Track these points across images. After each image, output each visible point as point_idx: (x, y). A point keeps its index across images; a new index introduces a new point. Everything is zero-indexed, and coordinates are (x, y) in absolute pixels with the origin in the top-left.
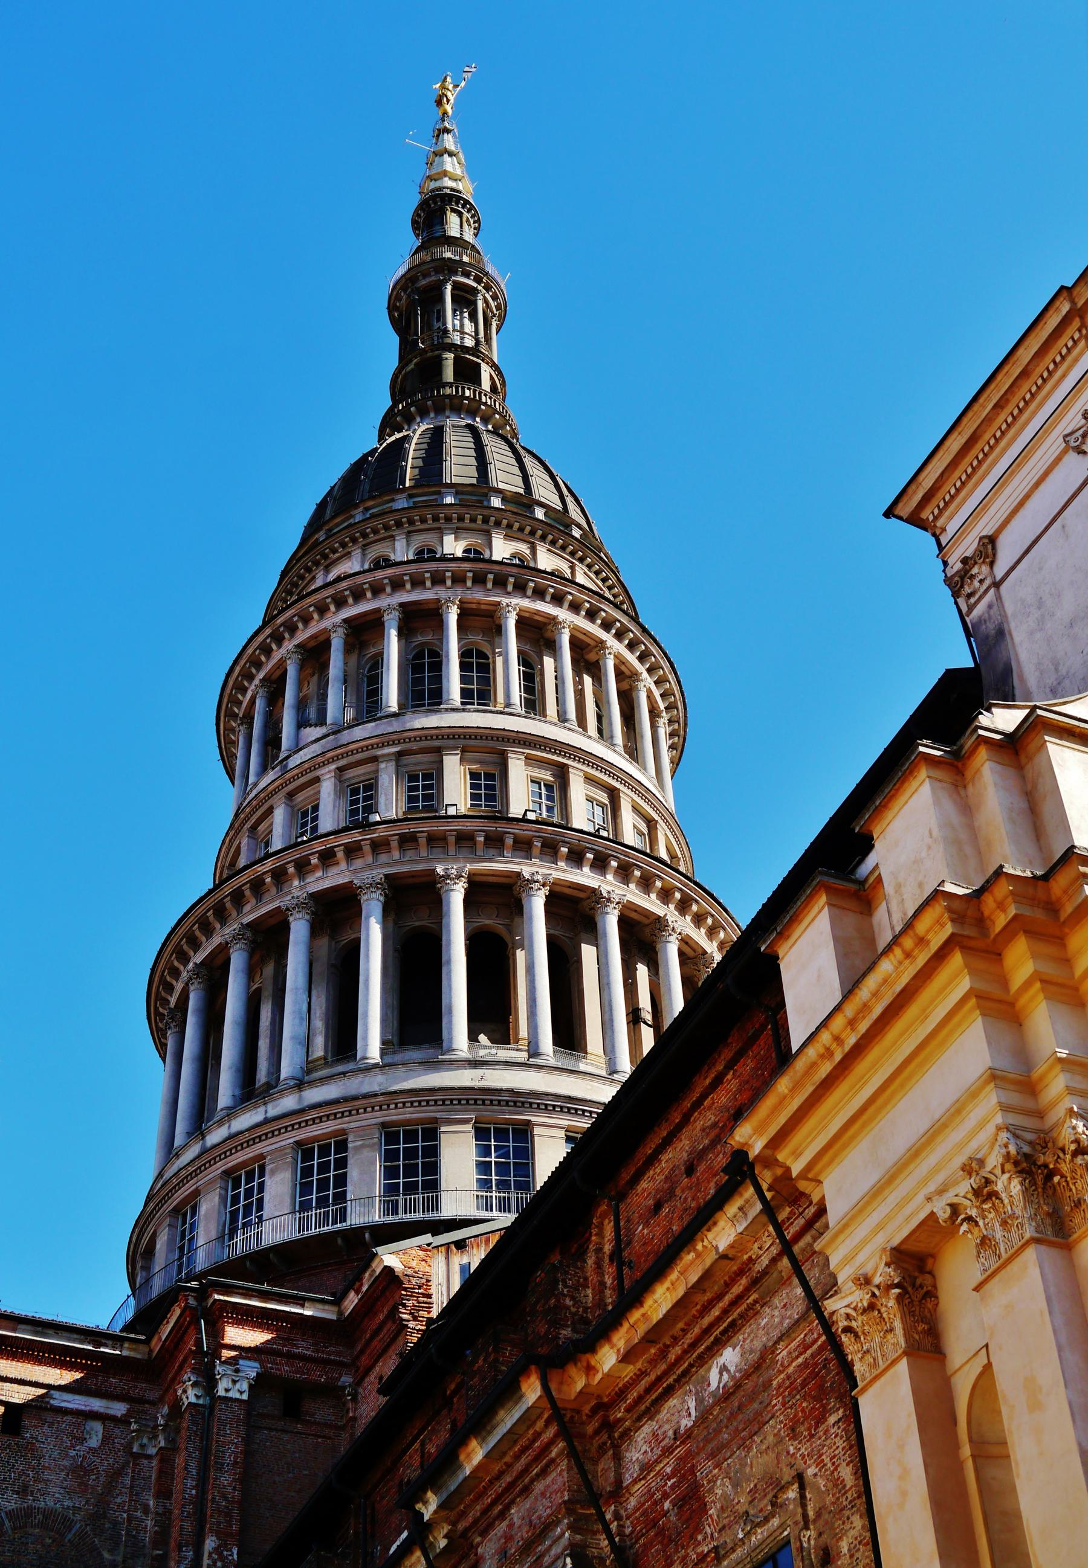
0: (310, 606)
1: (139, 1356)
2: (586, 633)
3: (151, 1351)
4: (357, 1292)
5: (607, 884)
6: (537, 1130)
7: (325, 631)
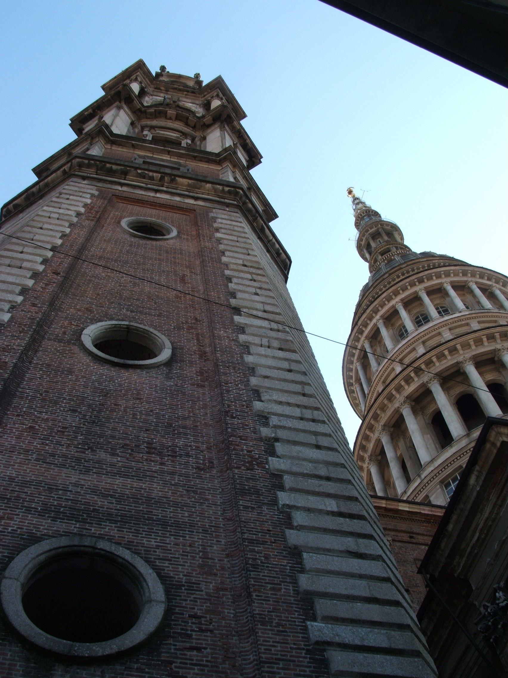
2: (458, 282)
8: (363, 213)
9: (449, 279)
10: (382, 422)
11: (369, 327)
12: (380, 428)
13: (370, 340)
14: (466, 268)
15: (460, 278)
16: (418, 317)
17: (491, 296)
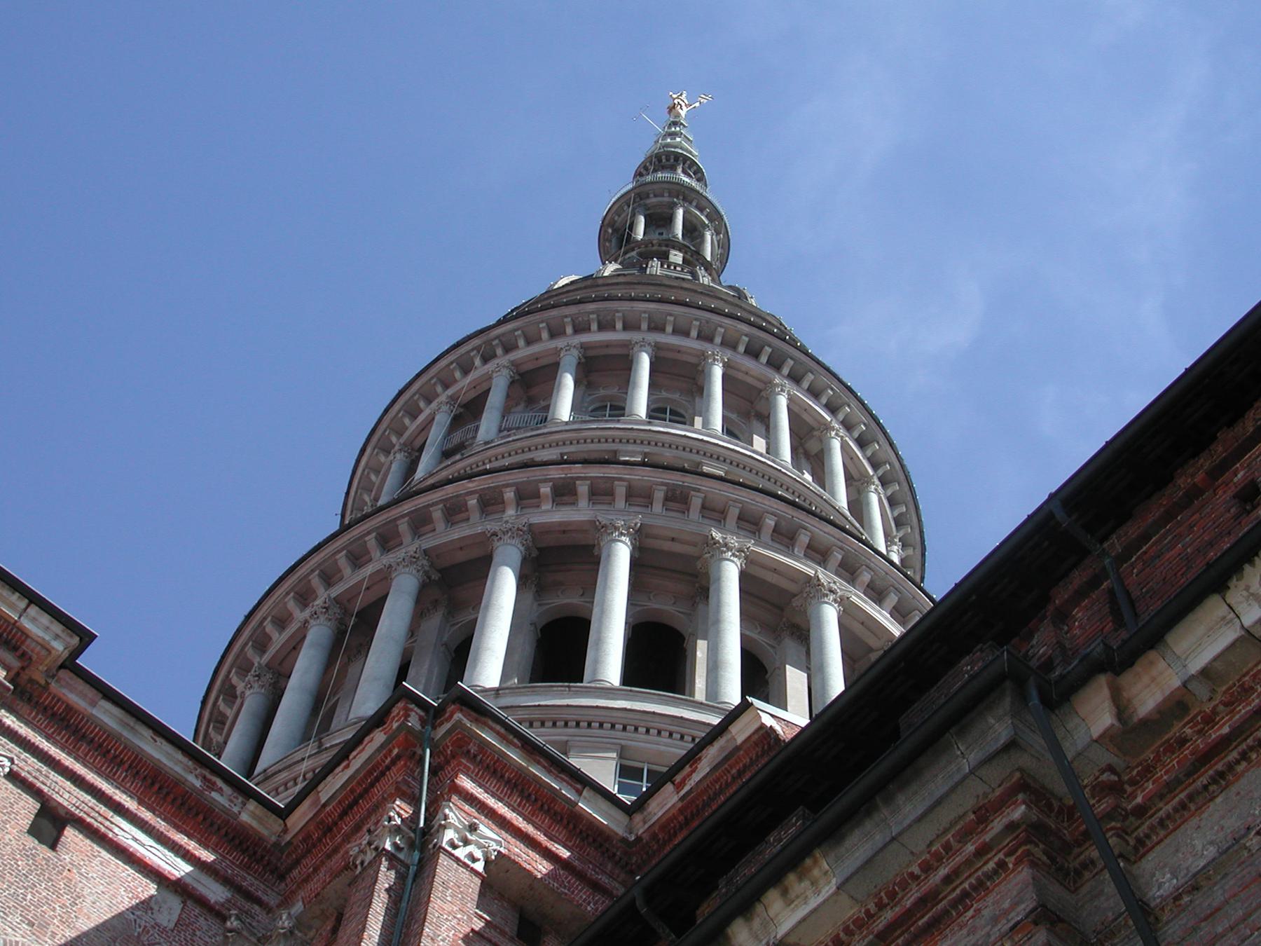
0: (542, 322)
1: (265, 832)
3: (285, 830)
4: (679, 787)
7: (557, 352)
8: (668, 160)
10: (428, 542)
11: (536, 348)
12: (412, 548)
13: (517, 377)
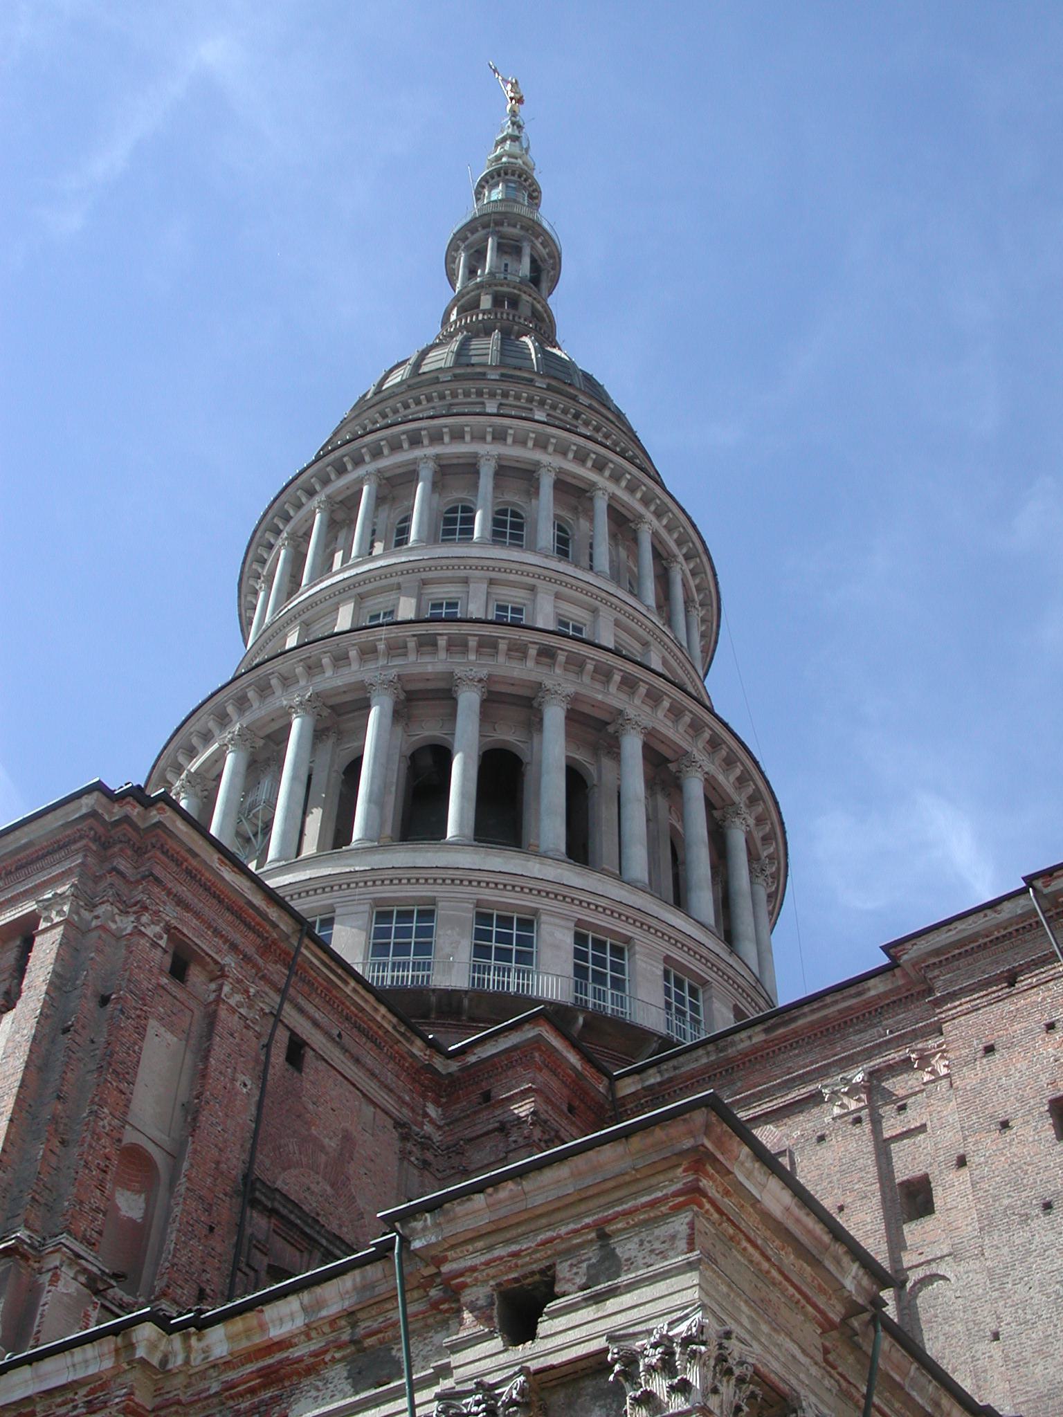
5: (635, 708)
6: (544, 918)
9: (612, 487)
14: (658, 490)
15: (633, 502)
16: (454, 510)
17: (664, 579)
